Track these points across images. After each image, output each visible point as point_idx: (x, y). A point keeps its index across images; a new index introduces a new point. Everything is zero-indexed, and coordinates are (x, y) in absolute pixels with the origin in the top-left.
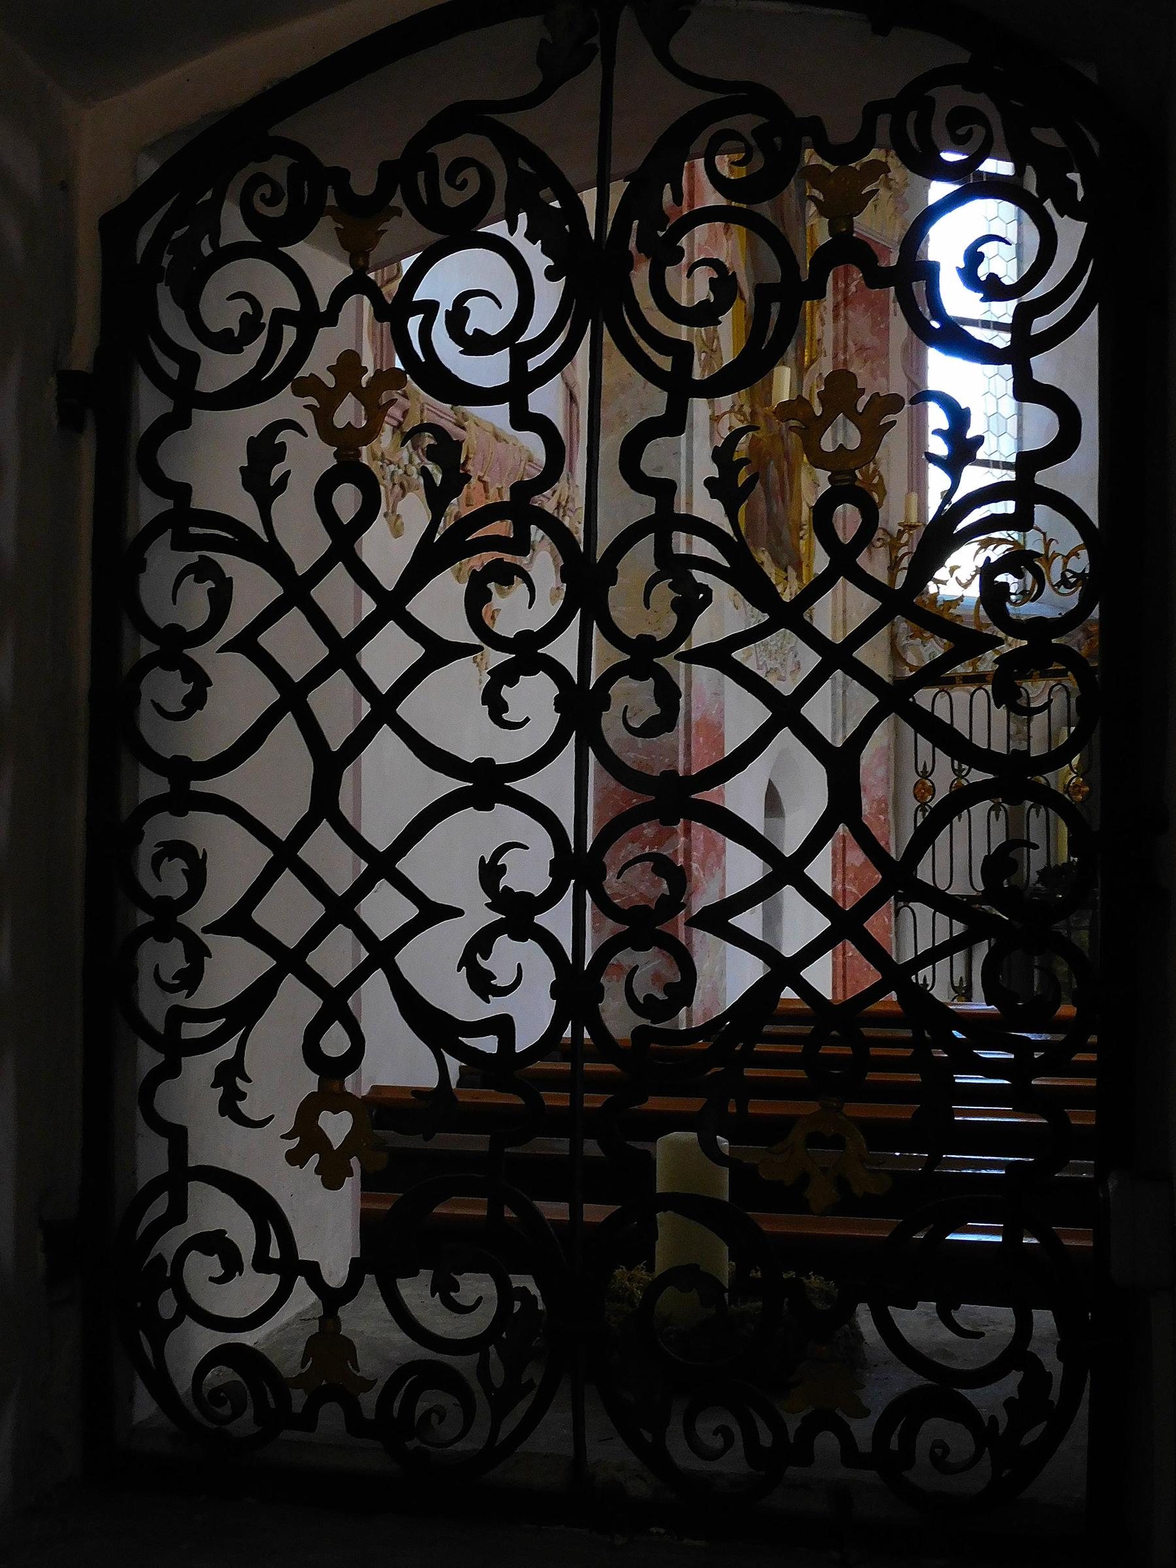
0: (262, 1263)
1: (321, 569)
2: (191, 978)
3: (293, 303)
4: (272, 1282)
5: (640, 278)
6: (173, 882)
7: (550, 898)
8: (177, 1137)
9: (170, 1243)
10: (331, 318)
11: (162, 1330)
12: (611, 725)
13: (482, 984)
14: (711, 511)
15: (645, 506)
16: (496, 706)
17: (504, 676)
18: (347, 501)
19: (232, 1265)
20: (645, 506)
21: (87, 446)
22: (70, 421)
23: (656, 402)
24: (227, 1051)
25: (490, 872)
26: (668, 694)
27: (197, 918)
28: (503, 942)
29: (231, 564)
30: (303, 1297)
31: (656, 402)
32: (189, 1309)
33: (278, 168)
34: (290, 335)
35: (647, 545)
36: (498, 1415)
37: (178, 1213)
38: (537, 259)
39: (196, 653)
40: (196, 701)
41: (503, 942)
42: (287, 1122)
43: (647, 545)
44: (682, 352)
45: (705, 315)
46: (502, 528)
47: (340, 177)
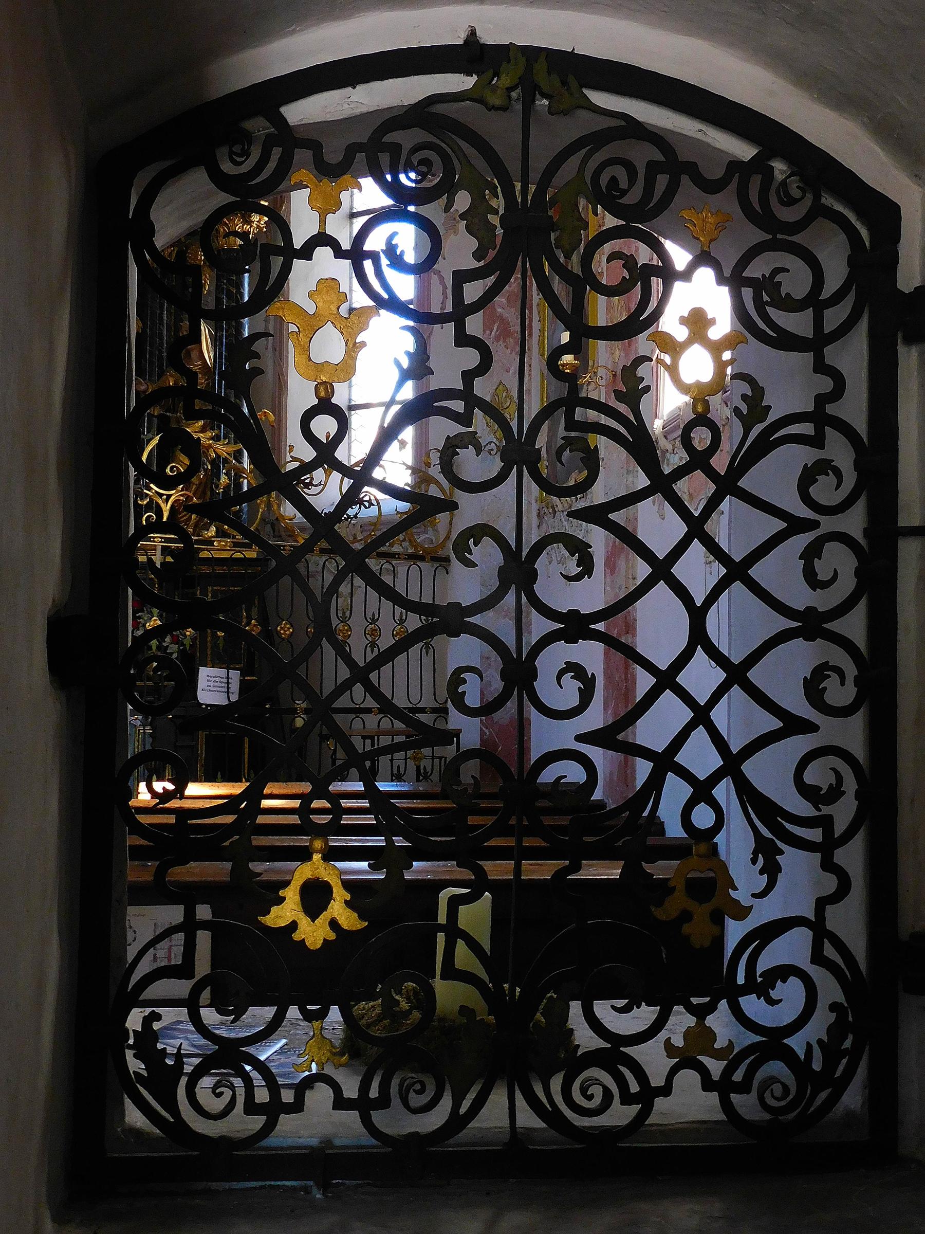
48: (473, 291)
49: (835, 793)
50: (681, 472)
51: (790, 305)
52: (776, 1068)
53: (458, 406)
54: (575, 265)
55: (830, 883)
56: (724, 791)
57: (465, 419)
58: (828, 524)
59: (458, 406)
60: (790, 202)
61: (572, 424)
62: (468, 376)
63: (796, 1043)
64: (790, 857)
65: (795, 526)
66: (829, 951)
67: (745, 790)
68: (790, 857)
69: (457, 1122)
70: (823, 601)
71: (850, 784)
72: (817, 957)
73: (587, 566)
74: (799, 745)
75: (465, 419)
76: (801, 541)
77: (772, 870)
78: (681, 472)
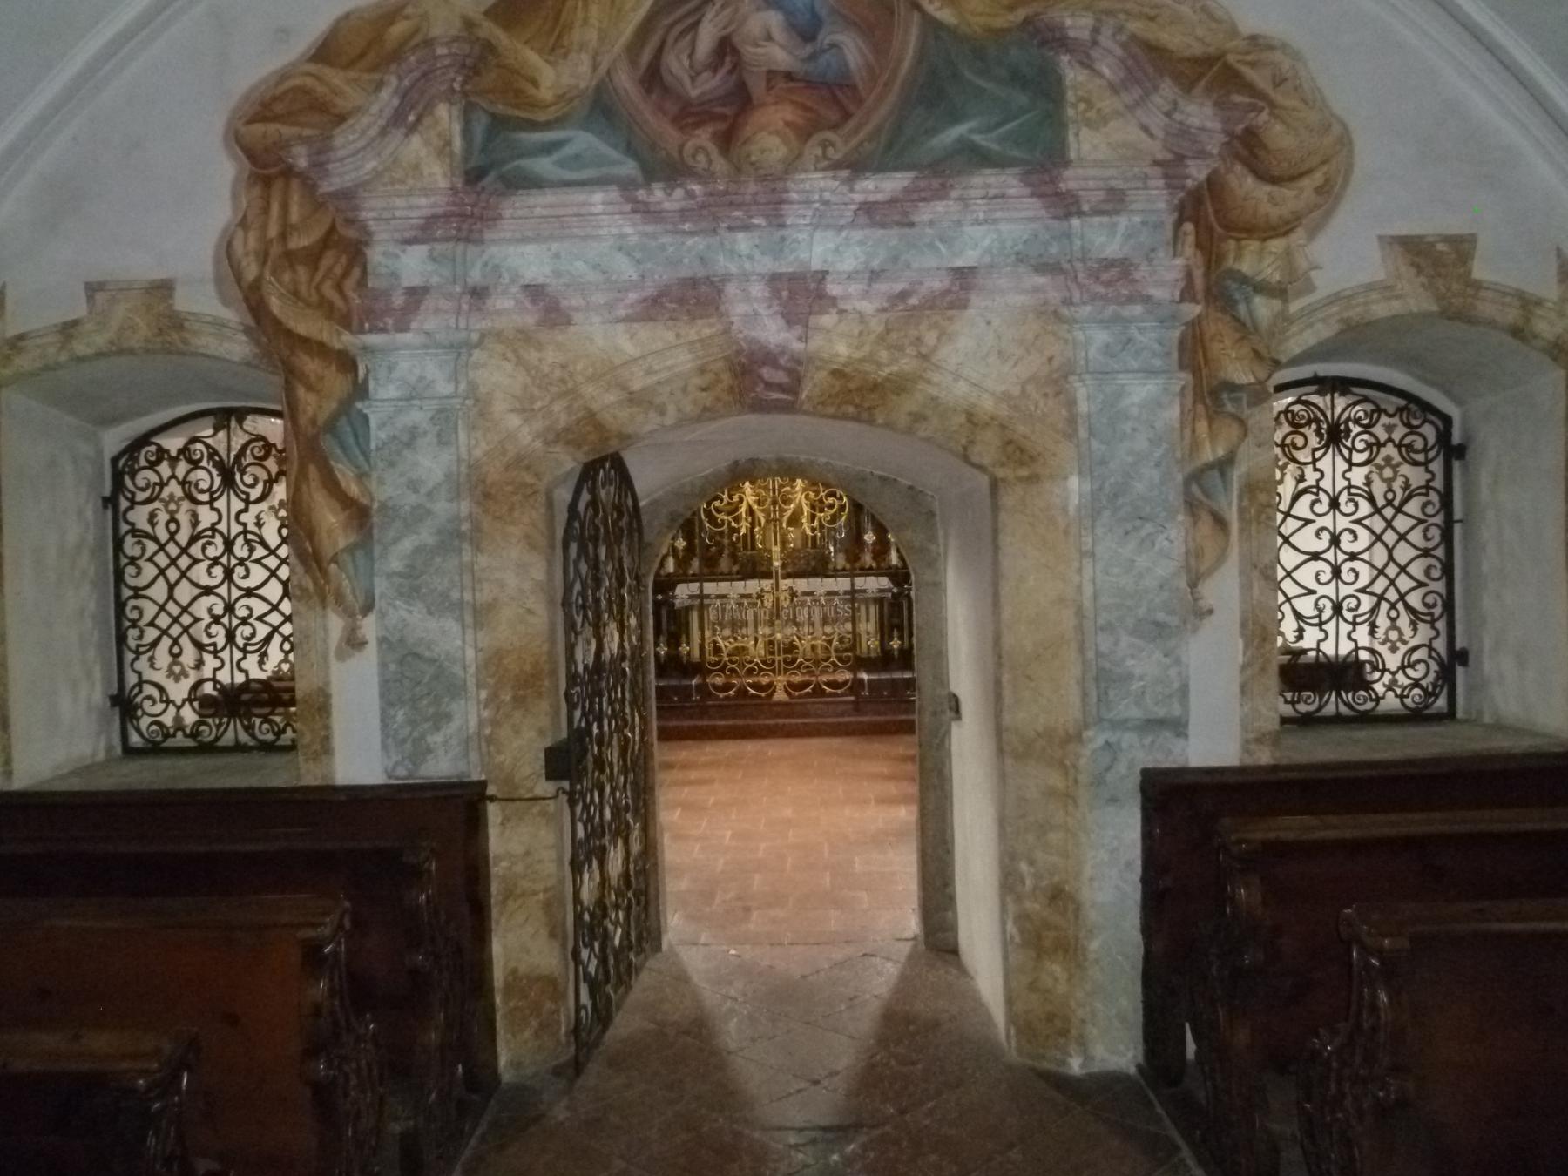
0: (162, 701)
1: (167, 542)
2: (141, 637)
3: (157, 480)
4: (164, 705)
5: (238, 477)
6: (135, 615)
7: (223, 616)
8: (139, 674)
9: (138, 700)
10: (167, 484)
11: (138, 719)
12: (235, 576)
13: (209, 635)
14: (256, 530)
15: (240, 528)
16: (209, 573)
17: (211, 566)
18: (173, 527)
19: (154, 702)
20: (240, 528)
21: (109, 513)
22: (105, 507)
23: (242, 505)
24: (150, 654)
25: (210, 610)
26: (247, 570)
27: (141, 623)
28: (213, 626)
29: (146, 541)
30: (172, 709)
31: (242, 505)
32: (145, 713)
33: (153, 448)
34: (157, 488)
35: (241, 537)
36: (218, 729)
37: (140, 691)
38: (215, 472)
39: (139, 562)
40: (139, 574)
41: (213, 626)
42: (165, 667)
43: (241, 537)
44: (248, 495)
45: (252, 486)
46: (209, 533)
47: (167, 452)
48: (1318, 454)
49: (1435, 605)
50: (1384, 507)
51: (1417, 452)
52: (1416, 691)
53: (1314, 490)
54: (1349, 444)
55: (1433, 633)
56: (1400, 606)
57: (1317, 494)
58: (1431, 520)
59: (1314, 490)
60: (1415, 418)
61: (1350, 494)
62: (1318, 481)
63: (1423, 683)
64: (1421, 626)
65: (1420, 522)
66: (1434, 654)
67: (1408, 607)
68: (1421, 626)
69: (1320, 708)
70: (1430, 545)
71: (1439, 602)
72: (1430, 656)
73: (1356, 537)
74: (1422, 591)
75: (1317, 494)
76: (1421, 527)
77: (1415, 629)
78: (1384, 507)
